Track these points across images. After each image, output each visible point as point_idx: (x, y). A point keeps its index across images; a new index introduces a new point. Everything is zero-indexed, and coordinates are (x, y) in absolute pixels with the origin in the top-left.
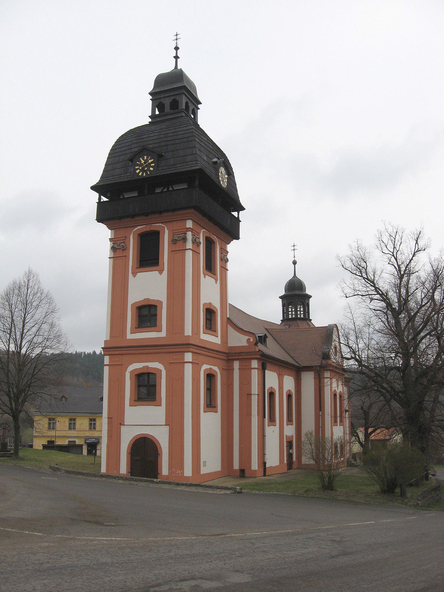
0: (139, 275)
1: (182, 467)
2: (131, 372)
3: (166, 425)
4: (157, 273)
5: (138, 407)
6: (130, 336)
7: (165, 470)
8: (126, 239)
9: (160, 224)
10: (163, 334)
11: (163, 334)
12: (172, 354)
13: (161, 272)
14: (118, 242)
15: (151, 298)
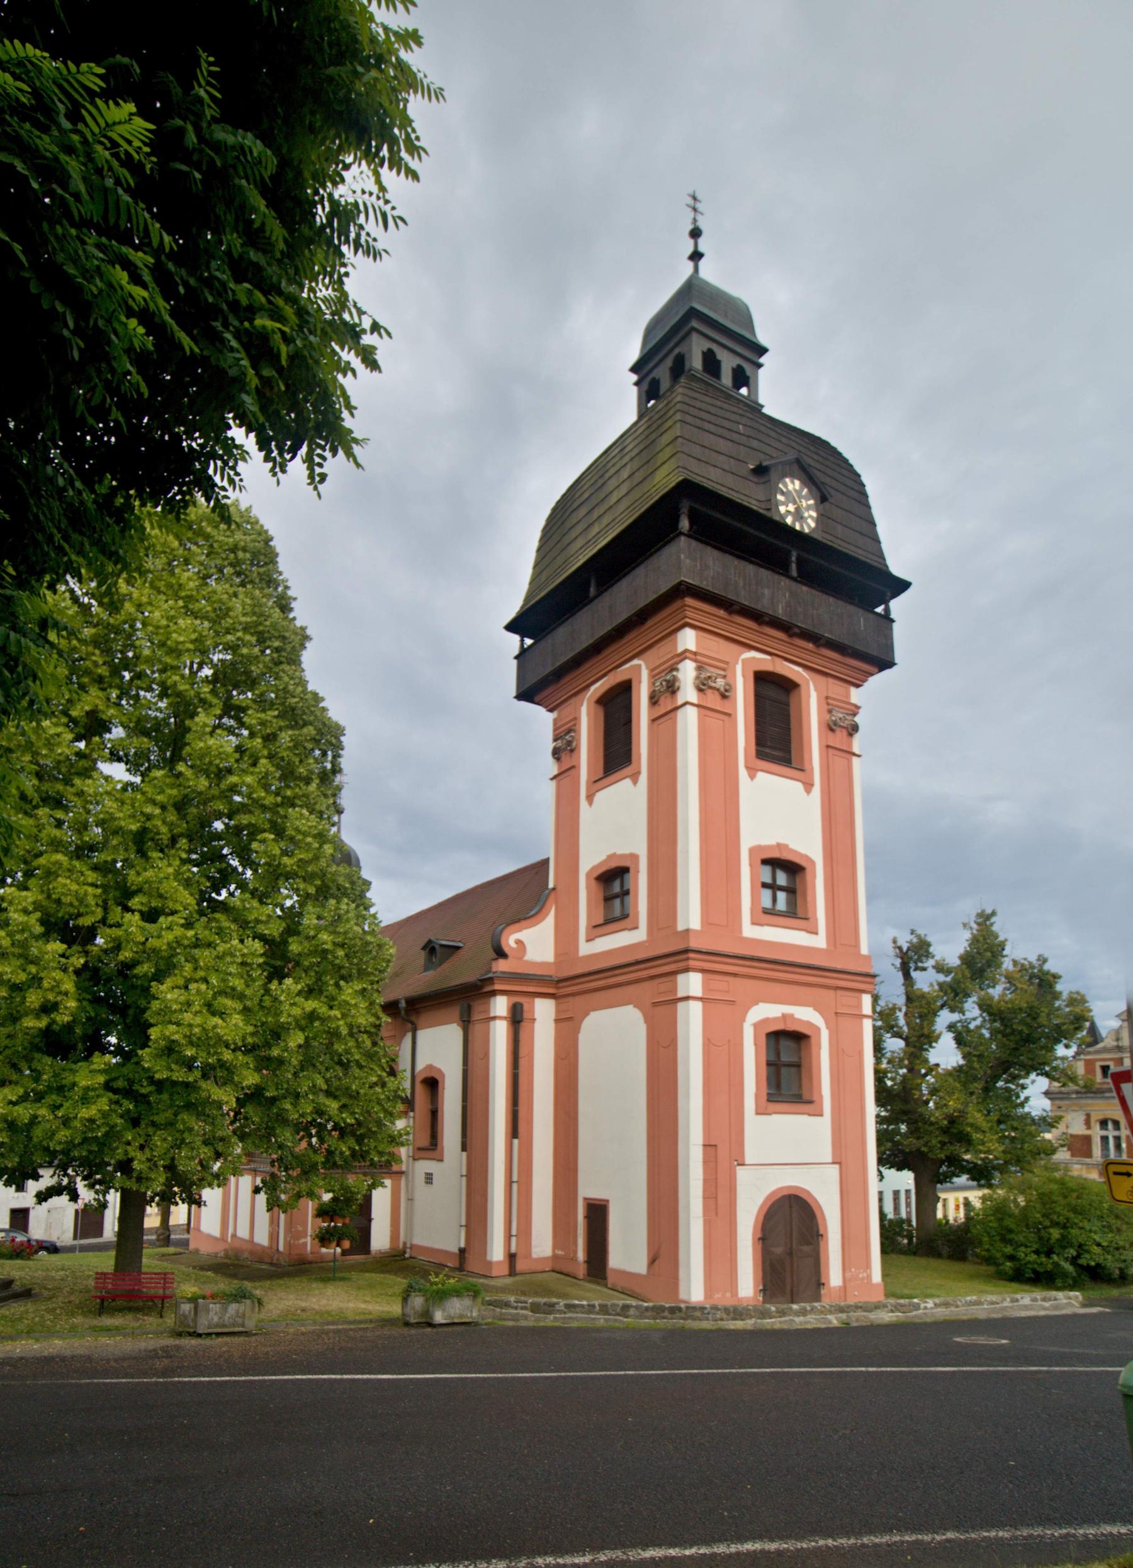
0: (761, 775)
1: (868, 1265)
2: (756, 1026)
3: (833, 1163)
4: (799, 786)
5: (774, 1116)
6: (749, 931)
7: (834, 1276)
8: (725, 668)
9: (799, 669)
10: (820, 941)
11: (820, 941)
12: (840, 993)
13: (808, 786)
14: (713, 670)
15: (793, 846)
